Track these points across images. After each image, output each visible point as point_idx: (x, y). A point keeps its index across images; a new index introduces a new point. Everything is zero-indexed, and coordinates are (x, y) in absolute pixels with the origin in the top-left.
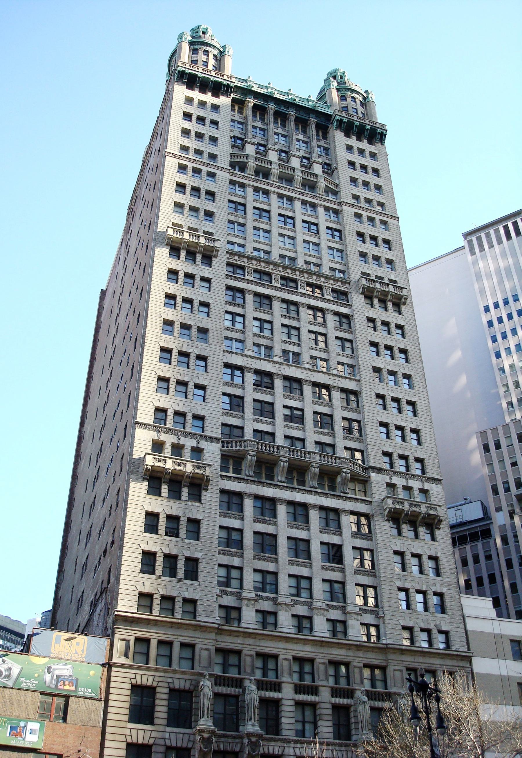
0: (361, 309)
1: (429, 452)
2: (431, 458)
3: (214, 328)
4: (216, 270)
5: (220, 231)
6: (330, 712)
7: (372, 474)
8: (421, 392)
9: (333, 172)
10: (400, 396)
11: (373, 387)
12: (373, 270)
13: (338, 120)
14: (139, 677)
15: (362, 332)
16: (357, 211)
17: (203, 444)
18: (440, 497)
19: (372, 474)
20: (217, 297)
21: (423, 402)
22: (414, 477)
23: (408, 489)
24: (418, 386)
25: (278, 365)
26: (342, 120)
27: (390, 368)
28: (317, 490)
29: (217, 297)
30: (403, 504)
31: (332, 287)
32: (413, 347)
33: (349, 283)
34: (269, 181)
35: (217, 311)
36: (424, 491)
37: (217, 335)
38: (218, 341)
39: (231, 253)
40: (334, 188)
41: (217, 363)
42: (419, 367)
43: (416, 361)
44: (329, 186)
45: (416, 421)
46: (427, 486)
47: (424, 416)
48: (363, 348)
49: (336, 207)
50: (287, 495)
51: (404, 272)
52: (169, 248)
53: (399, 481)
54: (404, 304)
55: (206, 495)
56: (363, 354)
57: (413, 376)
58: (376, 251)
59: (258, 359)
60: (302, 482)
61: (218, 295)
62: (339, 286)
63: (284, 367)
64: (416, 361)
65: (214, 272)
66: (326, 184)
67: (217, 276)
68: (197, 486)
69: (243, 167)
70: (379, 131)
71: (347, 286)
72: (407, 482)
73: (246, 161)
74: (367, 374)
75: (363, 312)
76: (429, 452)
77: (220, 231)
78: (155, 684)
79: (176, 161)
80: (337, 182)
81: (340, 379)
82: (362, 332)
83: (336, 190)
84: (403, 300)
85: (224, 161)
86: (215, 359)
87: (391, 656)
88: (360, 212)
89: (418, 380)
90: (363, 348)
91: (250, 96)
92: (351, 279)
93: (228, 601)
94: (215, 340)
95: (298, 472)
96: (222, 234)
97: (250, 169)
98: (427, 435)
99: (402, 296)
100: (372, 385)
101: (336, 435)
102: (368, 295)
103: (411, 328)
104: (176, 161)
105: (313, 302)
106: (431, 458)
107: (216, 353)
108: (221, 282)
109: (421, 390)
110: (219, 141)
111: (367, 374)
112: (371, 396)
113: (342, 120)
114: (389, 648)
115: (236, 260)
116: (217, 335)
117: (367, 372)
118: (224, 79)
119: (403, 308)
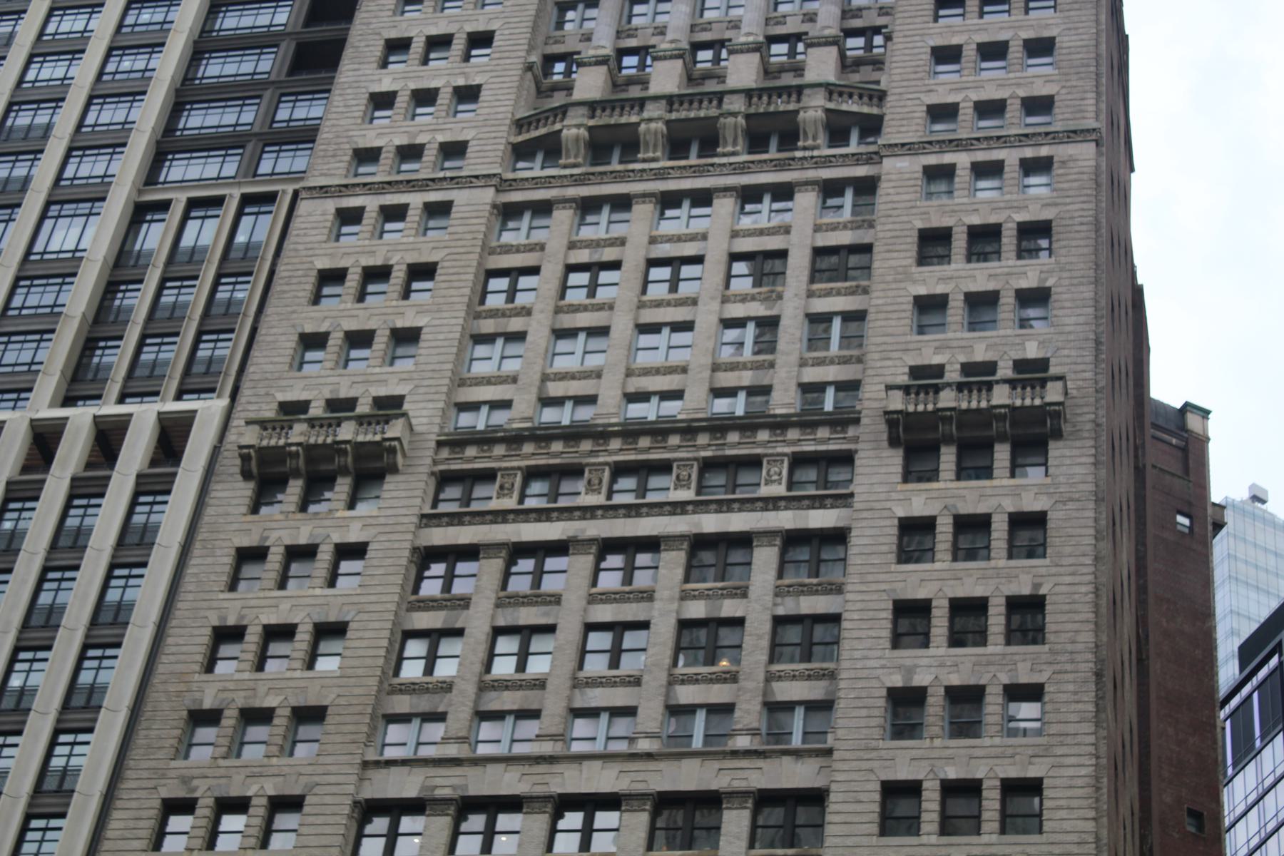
0: (883, 496)
3: (342, 701)
5: (426, 383)
8: (1069, 740)
10: (979, 771)
11: (875, 764)
12: (953, 346)
15: (870, 578)
16: (932, 160)
20: (373, 598)
21: (1071, 772)
24: (1061, 717)
25: (542, 768)
27: (955, 680)
29: (373, 598)
31: (788, 450)
32: (1068, 579)
33: (857, 421)
35: (365, 643)
37: (348, 719)
38: (349, 738)
39: (456, 442)
40: (866, 110)
41: (328, 810)
42: (1080, 647)
43: (1069, 626)
44: (844, 107)
47: (1067, 826)
48: (863, 634)
49: (861, 171)
51: (1082, 319)
52: (251, 485)
54: (1058, 434)
56: (857, 654)
57: (1047, 688)
58: (981, 277)
61: (380, 589)
62: (823, 441)
63: (557, 768)
64: (1069, 626)
66: (831, 106)
67: (388, 529)
69: (551, 148)
71: (851, 432)
73: (557, 126)
74: (863, 723)
75: (888, 505)
77: (426, 383)
79: (330, 206)
80: (883, 86)
81: (760, 763)
82: (870, 578)
83: (875, 111)
85: (488, 153)
86: (328, 799)
88: (948, 158)
89: (1063, 697)
90: (863, 634)
92: (866, 404)
94: (338, 738)
96: (433, 390)
100: (874, 754)
102: (917, 442)
103: (1075, 514)
104: (330, 206)
105: (711, 523)
107: (332, 779)
108: (396, 545)
109: (1071, 729)
110: (484, 95)
111: (863, 723)
112: (862, 797)
116: (348, 719)
117: (864, 712)
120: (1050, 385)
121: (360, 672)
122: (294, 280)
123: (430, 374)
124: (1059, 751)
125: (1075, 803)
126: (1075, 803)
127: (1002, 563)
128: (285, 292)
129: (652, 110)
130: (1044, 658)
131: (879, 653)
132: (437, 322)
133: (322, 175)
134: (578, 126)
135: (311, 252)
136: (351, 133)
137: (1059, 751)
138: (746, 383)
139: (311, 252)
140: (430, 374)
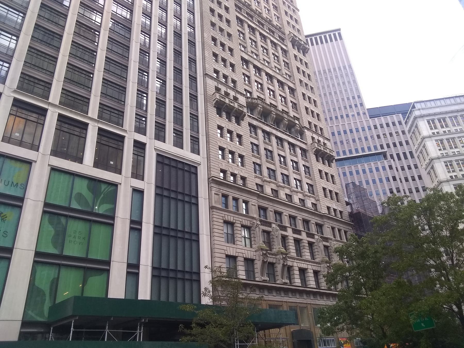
6: (307, 245)
14: (226, 216)
17: (238, 96)
19: (306, 131)
23: (319, 141)
36: (325, 144)
50: (274, 132)
55: (243, 123)
68: (239, 117)
78: (234, 221)
84: (307, 50)
87: (325, 220)
93: (259, 181)
95: (278, 122)
99: (307, 48)
114: (325, 216)
119: (306, 55)
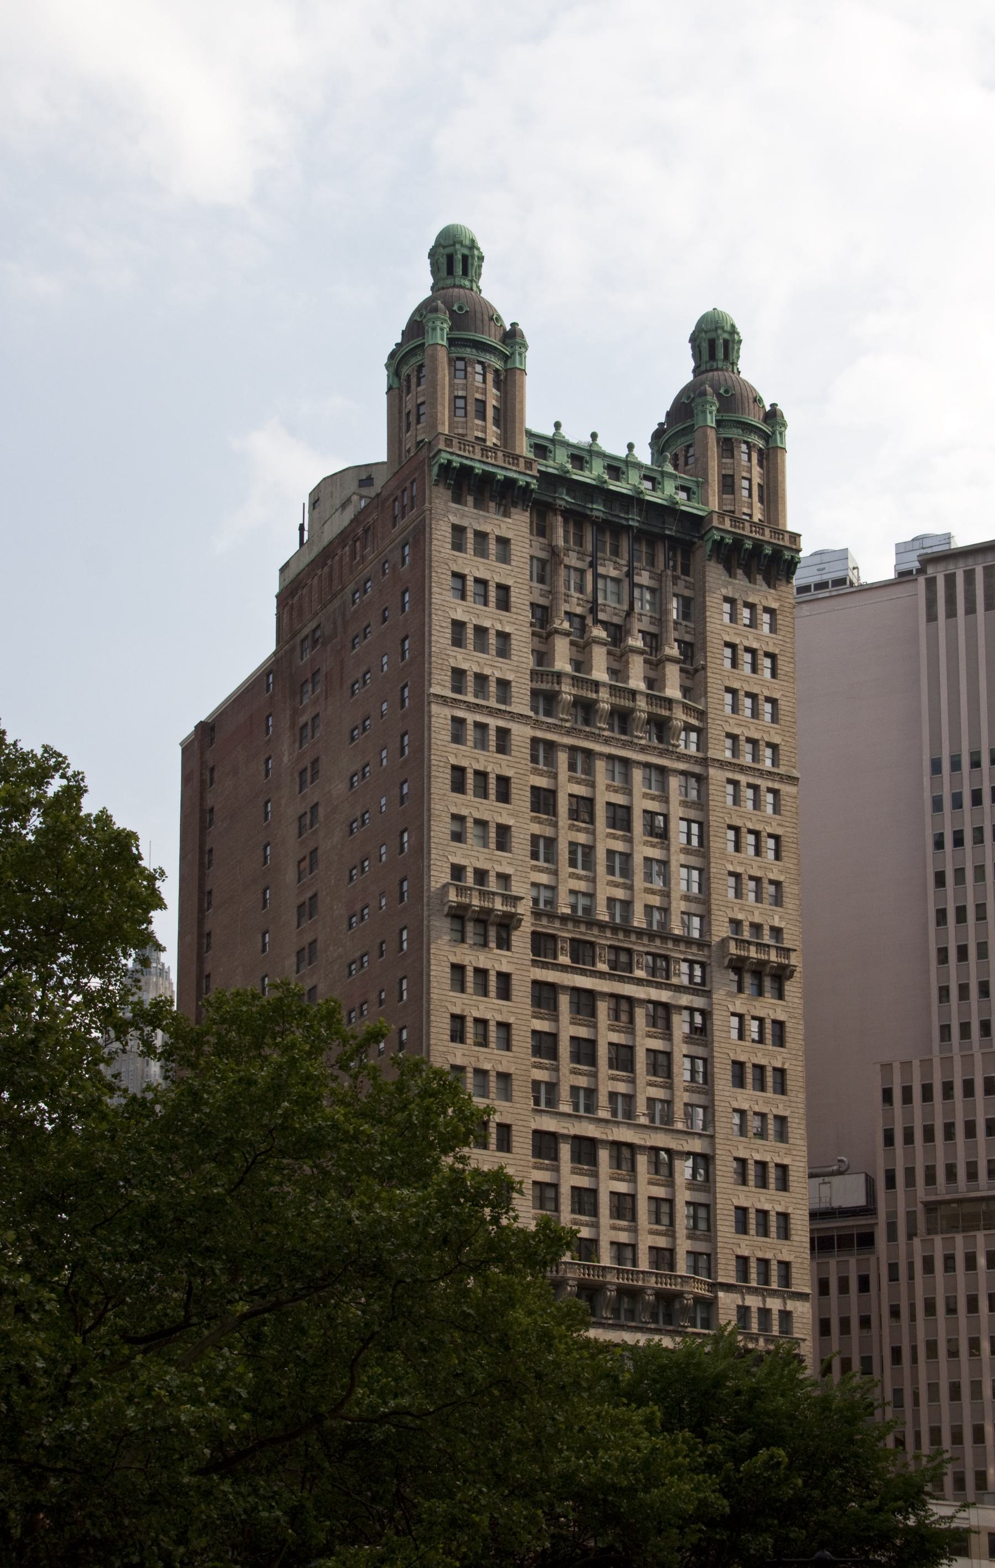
1: (799, 1249)
2: (800, 1260)
3: (518, 1072)
4: (517, 955)
7: (721, 1294)
9: (696, 671)
11: (730, 1148)
13: (715, 541)
18: (805, 1321)
19: (721, 1294)
22: (774, 1293)
26: (722, 538)
28: (649, 1326)
30: (757, 1340)
34: (594, 730)
42: (799, 1100)
45: (786, 1199)
46: (791, 1305)
53: (753, 1302)
59: (577, 1116)
60: (632, 1315)
63: (610, 1126)
65: (515, 960)
70: (787, 555)
72: (764, 1304)
76: (799, 1249)
91: (560, 490)
97: (564, 708)
98: (799, 1222)
99: (788, 966)
100: (729, 1143)
101: (677, 1235)
106: (800, 1260)
113: (722, 538)
115: (546, 926)
118: (520, 473)
120: (791, 953)
121: (522, 1056)
122: (441, 770)
123: (520, 863)
124: (794, 1152)
125: (800, 1180)
126: (800, 1180)
127: (770, 1048)
128: (438, 777)
129: (604, 694)
130: (788, 1103)
131: (728, 1088)
132: (518, 825)
133: (438, 684)
134: (570, 694)
135: (444, 749)
136: (448, 652)
137: (794, 1152)
138: (658, 905)
139: (444, 749)
140: (520, 863)
